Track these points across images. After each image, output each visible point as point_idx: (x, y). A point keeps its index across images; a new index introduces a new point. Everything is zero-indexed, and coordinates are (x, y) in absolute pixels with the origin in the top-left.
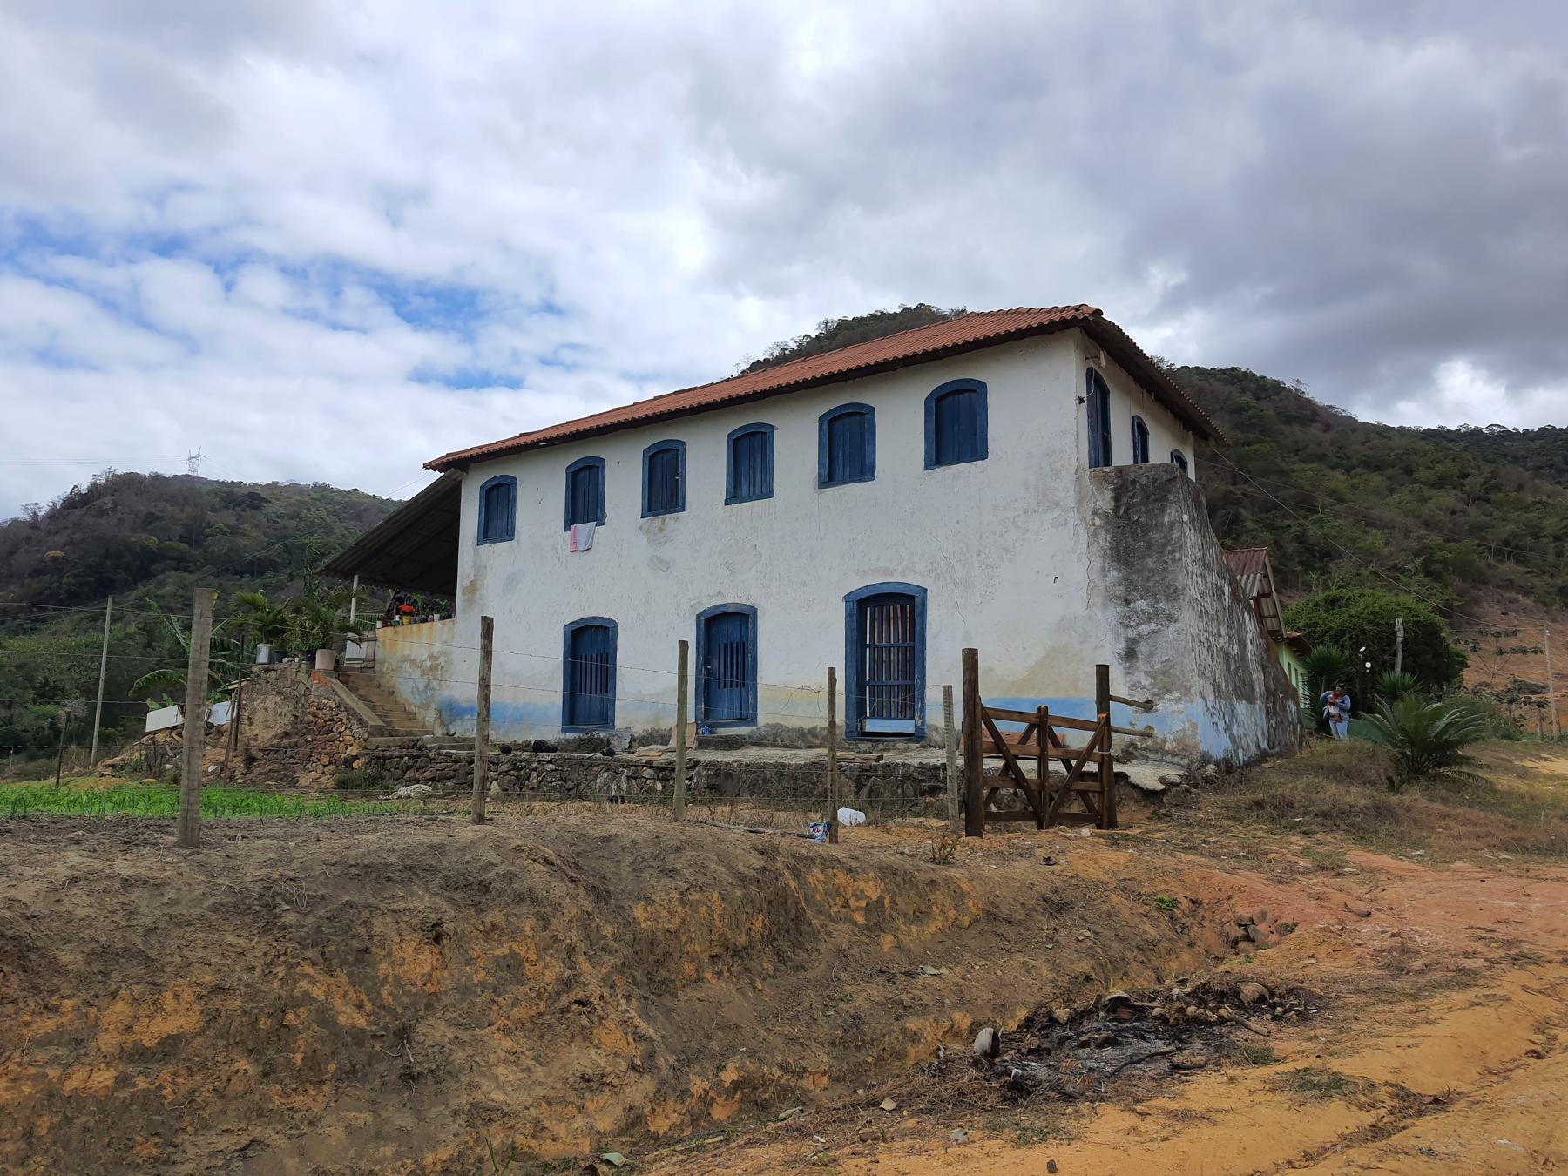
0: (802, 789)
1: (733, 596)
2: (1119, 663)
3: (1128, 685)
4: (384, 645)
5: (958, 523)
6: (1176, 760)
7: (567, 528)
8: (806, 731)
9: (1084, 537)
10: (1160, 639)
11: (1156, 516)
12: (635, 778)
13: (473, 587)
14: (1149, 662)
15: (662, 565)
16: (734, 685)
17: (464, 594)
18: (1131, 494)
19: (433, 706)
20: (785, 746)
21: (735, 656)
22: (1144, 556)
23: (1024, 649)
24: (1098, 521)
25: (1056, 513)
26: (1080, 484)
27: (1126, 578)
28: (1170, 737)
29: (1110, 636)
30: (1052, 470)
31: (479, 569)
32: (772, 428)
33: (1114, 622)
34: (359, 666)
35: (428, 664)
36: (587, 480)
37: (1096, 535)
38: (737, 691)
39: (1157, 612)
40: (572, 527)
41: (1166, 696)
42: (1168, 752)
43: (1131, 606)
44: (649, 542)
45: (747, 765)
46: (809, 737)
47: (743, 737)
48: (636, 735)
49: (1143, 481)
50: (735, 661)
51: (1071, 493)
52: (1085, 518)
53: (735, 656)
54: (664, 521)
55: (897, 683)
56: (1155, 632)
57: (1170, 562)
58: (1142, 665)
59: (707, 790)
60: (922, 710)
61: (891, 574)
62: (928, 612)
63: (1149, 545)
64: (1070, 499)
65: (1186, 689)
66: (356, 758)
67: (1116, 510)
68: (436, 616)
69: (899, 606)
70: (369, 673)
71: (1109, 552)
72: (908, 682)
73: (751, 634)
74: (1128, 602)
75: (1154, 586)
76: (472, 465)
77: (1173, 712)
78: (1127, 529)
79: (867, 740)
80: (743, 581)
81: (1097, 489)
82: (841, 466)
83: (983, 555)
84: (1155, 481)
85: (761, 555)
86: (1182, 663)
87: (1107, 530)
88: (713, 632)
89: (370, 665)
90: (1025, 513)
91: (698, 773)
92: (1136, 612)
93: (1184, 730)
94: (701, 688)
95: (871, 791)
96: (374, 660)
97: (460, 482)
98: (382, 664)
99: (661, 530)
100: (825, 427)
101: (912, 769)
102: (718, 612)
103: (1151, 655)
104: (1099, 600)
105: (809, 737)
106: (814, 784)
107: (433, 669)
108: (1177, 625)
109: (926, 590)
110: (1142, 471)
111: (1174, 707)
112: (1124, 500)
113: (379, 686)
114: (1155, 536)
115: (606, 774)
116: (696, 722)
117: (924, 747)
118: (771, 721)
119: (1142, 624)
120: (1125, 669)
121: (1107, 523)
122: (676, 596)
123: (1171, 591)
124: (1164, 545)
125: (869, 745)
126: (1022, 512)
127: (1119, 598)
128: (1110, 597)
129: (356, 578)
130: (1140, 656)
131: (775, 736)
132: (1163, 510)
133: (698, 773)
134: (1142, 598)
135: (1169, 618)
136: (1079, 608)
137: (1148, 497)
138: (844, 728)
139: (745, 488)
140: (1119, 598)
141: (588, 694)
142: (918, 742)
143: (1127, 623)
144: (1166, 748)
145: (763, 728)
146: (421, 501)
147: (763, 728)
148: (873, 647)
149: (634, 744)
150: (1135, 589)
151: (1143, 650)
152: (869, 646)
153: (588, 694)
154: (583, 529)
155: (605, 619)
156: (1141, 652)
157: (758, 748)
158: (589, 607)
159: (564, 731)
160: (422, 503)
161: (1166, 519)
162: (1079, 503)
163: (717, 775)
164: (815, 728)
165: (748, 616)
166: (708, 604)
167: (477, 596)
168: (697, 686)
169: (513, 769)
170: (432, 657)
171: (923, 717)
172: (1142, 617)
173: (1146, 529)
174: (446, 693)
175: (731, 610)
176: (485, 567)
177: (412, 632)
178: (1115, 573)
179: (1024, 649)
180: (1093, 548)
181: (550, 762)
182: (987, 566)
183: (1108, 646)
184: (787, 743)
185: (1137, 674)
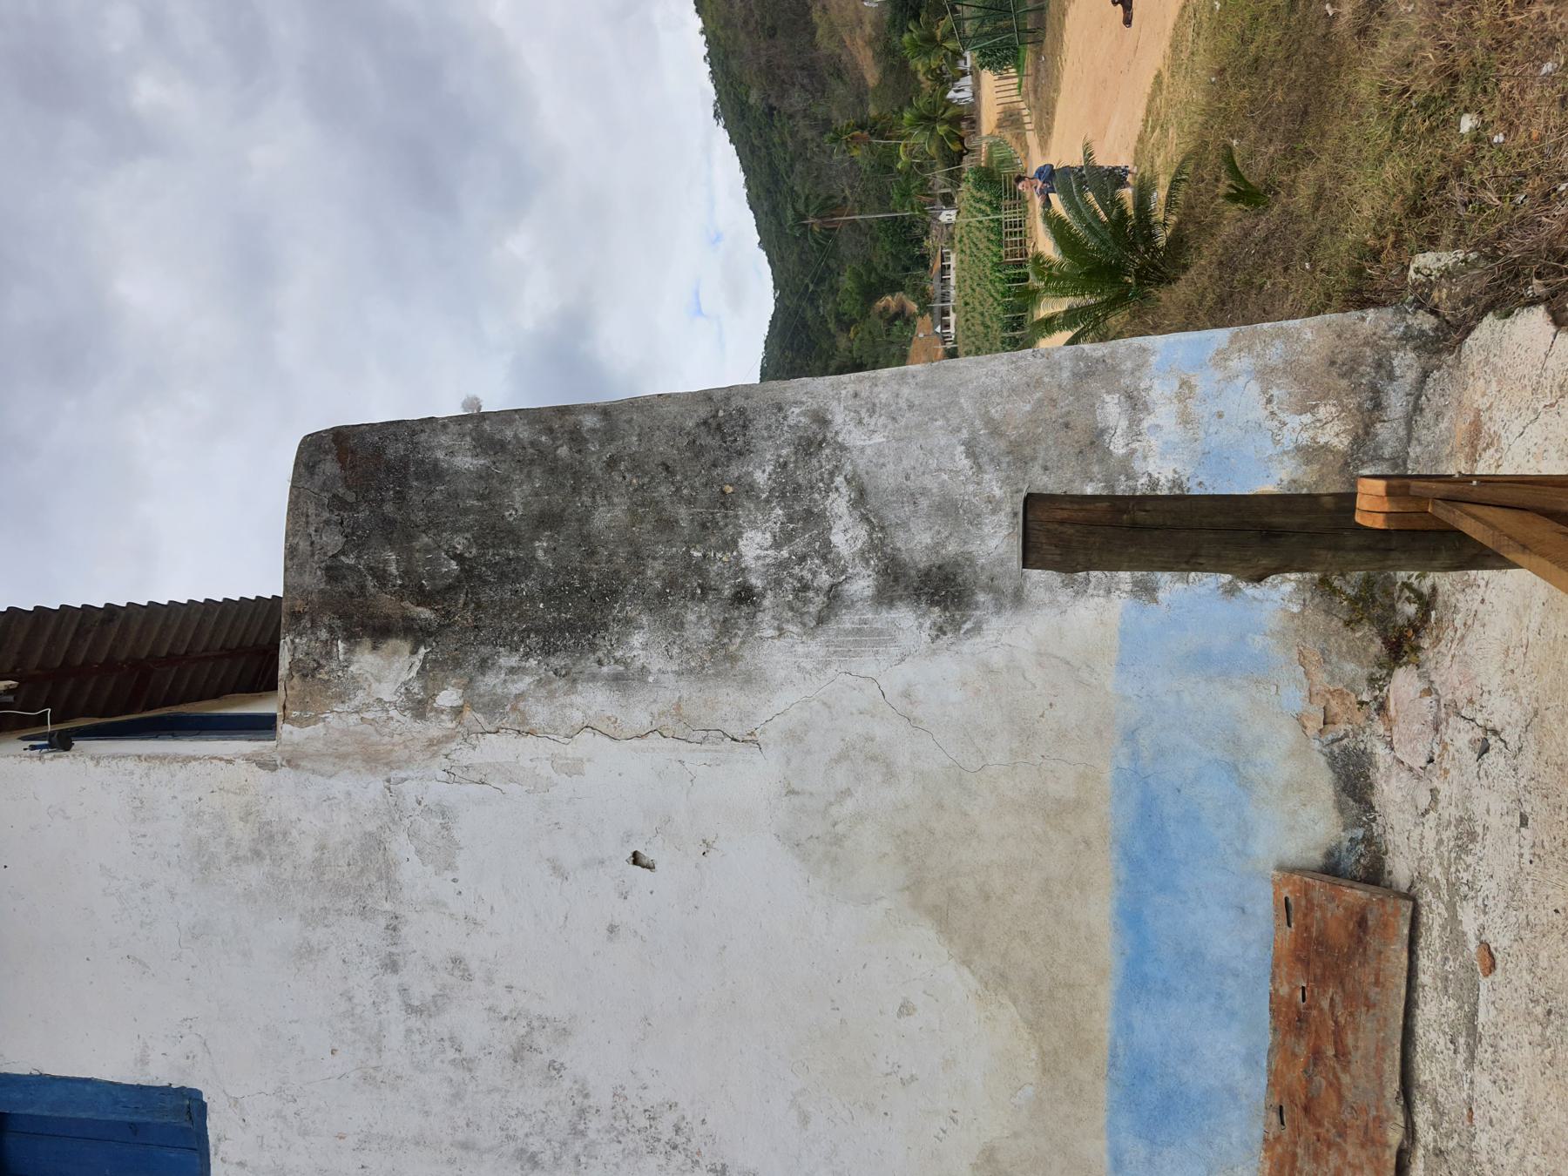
2: (977, 629)
6: (1396, 402)
9: (497, 748)
10: (888, 478)
11: (453, 496)
14: (976, 519)
18: (370, 583)
22: (586, 538)
23: (905, 1009)
24: (448, 697)
25: (400, 846)
26: (320, 756)
28: (1297, 428)
29: (868, 664)
30: (257, 854)
33: (816, 647)
37: (493, 706)
39: (787, 490)
41: (1118, 447)
42: (1363, 437)
43: (756, 582)
49: (332, 541)
51: (339, 785)
52: (431, 743)
56: (861, 497)
57: (611, 449)
63: (548, 520)
65: (1089, 374)
67: (417, 634)
71: (556, 661)
74: (745, 596)
75: (690, 502)
77: (1185, 420)
78: (486, 595)
81: (341, 697)
83: (535, 1144)
84: (338, 503)
86: (985, 394)
87: (484, 665)
90: (392, 965)
92: (782, 565)
93: (1265, 375)
103: (949, 510)
104: (727, 702)
108: (839, 417)
111: (1163, 415)
112: (387, 603)
119: (827, 544)
120: (999, 608)
121: (457, 664)
124: (554, 469)
126: (392, 980)
127: (726, 627)
130: (952, 548)
132: (434, 473)
134: (731, 544)
135: (809, 446)
137: (388, 523)
140: (726, 627)
143: (820, 600)
144: (1342, 443)
150: (699, 569)
151: (926, 539)
156: (936, 547)
161: (466, 462)
162: (373, 759)
172: (799, 545)
173: (494, 532)
178: (637, 639)
179: (905, 1009)
180: (539, 713)
182: (578, 1133)
183: (907, 670)
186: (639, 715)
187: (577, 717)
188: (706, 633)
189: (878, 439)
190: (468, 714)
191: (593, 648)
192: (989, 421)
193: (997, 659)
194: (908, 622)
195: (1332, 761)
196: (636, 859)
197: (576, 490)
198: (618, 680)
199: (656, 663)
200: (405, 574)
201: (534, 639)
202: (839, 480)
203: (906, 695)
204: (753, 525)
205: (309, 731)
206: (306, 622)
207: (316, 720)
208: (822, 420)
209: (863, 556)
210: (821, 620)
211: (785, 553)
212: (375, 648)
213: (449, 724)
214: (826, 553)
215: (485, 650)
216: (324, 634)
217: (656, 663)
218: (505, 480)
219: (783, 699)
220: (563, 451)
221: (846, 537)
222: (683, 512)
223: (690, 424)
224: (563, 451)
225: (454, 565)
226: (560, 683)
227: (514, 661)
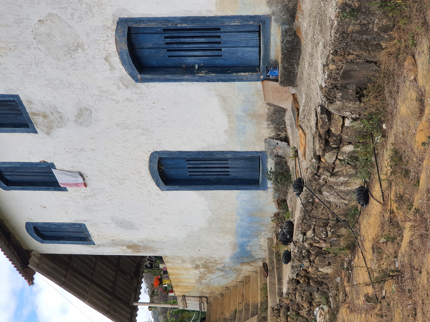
4: (188, 292)
12: (334, 168)
16: (218, 40)
17: (140, 252)
19: (238, 266)
21: (182, 40)
31: (115, 243)
34: (206, 305)
35: (202, 270)
36: (12, 174)
38: (224, 37)
40: (62, 186)
44: (61, 127)
45: (335, 53)
47: (285, 33)
48: (273, 134)
50: (188, 40)
53: (182, 40)
59: (364, 99)
68: (161, 266)
70: (211, 299)
73: (153, 25)
76: (24, 248)
80: (88, 35)
85: (50, 15)
88: (154, 63)
89: (204, 300)
91: (338, 110)
94: (221, 76)
96: (200, 297)
97: (41, 254)
99: (45, 116)
102: (129, 60)
107: (206, 266)
113: (222, 295)
115: (324, 193)
116: (263, 80)
122: (117, 102)
133: (338, 110)
141: (229, 162)
145: (274, 8)
146: (63, 279)
147: (274, 8)
149: (283, 135)
154: (61, 178)
155: (150, 161)
157: (299, 14)
158: (140, 173)
159: (265, 188)
160: (65, 277)
163: (344, 87)
165: (129, 28)
167: (140, 244)
168: (218, 81)
169: (309, 258)
170: (197, 267)
174: (227, 260)
175: (125, 47)
176: (113, 240)
177: (174, 274)
181: (304, 234)
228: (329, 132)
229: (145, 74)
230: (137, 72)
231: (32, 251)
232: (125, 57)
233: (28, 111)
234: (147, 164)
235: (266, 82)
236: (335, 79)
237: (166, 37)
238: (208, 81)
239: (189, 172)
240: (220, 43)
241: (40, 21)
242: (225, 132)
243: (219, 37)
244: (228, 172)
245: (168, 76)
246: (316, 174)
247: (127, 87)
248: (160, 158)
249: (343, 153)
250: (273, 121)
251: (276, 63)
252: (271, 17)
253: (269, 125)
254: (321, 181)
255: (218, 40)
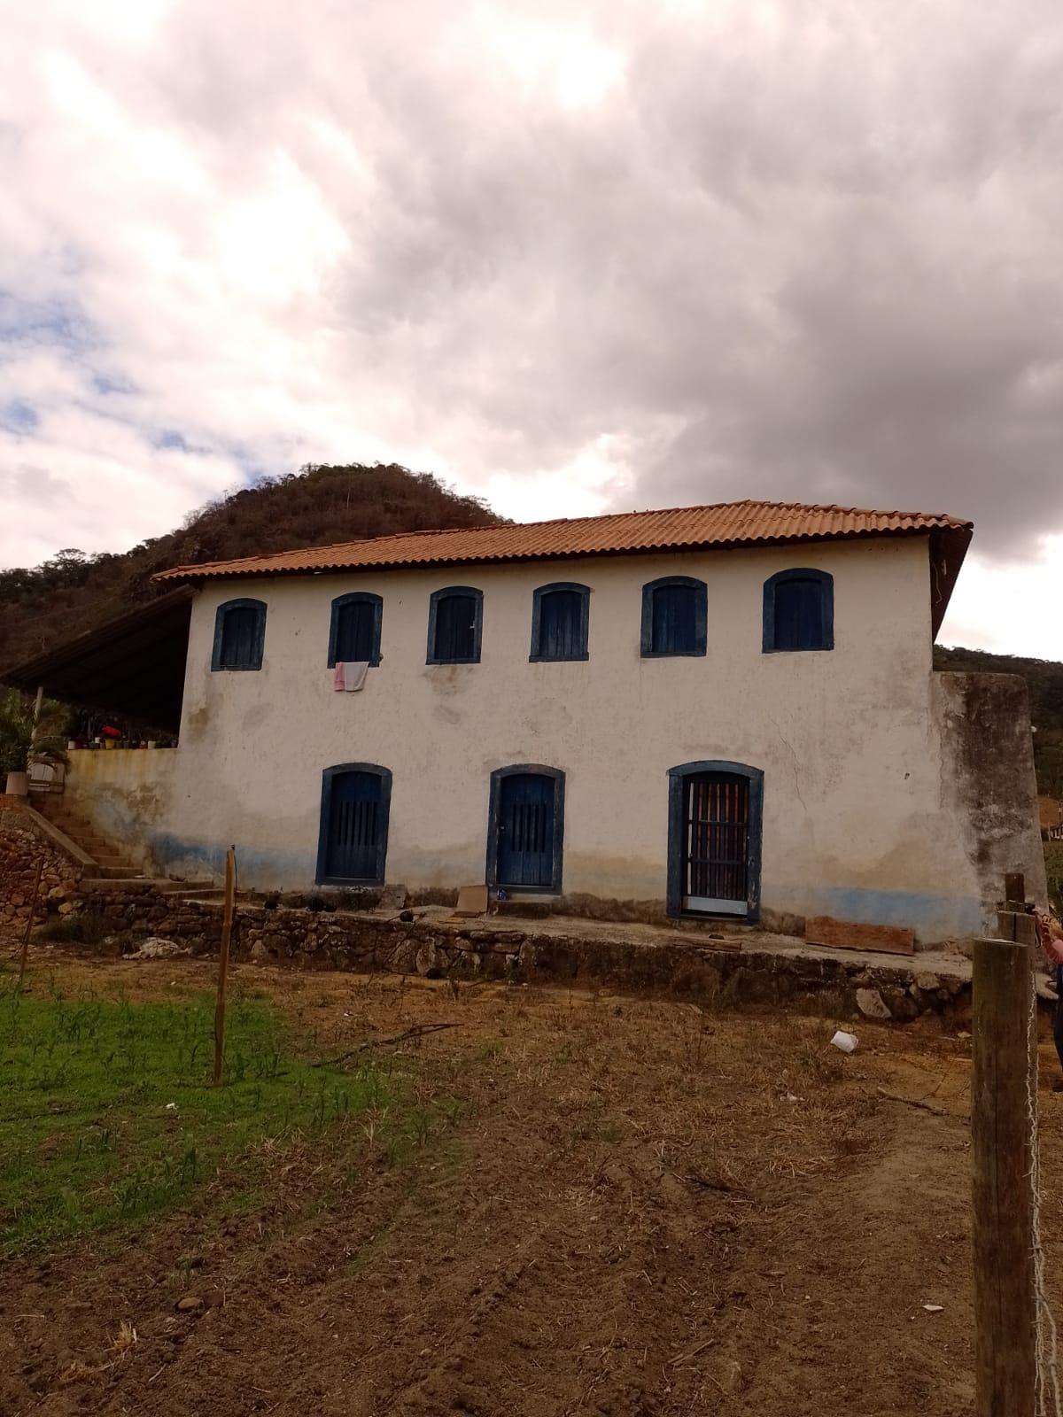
0: (658, 974)
1: (537, 755)
3: (981, 885)
5: (799, 709)
7: (331, 664)
8: (620, 905)
9: (937, 739)
13: (203, 716)
14: (1003, 865)
15: (454, 717)
16: (532, 848)
17: (191, 721)
20: (595, 918)
23: (872, 841)
24: (950, 724)
27: (978, 782)
29: (962, 836)
30: (904, 669)
31: (213, 697)
32: (588, 590)
33: (967, 824)
34: (42, 790)
35: (139, 795)
37: (948, 736)
39: (1009, 818)
40: (339, 665)
43: (984, 809)
46: (624, 910)
48: (411, 893)
49: (995, 690)
54: (454, 670)
55: (721, 862)
56: (1008, 837)
57: (1021, 770)
58: (996, 868)
60: (757, 893)
61: (723, 752)
62: (766, 795)
63: (1001, 752)
64: (925, 700)
65: (1039, 893)
66: (63, 900)
67: (968, 714)
68: (151, 743)
69: (727, 786)
71: (961, 754)
72: (736, 863)
74: (980, 805)
75: (1006, 792)
79: (692, 919)
81: (949, 692)
82: (665, 637)
87: (959, 733)
89: (57, 789)
90: (874, 707)
91: (526, 949)
92: (989, 815)
95: (740, 981)
97: (191, 599)
98: (75, 789)
100: (650, 596)
101: (788, 962)
102: (518, 772)
103: (1004, 859)
105: (624, 910)
106: (671, 969)
107: (145, 801)
108: (1029, 832)
109: (763, 772)
110: (993, 680)
112: (976, 706)
113: (69, 814)
114: (1007, 744)
115: (409, 942)
117: (758, 930)
118: (579, 891)
119: (994, 827)
120: (978, 870)
121: (960, 726)
123: (1023, 798)
125: (694, 923)
126: (870, 707)
127: (971, 800)
128: (962, 799)
129: (40, 691)
130: (994, 859)
131: (583, 907)
132: (1014, 720)
135: (1022, 824)
136: (931, 806)
138: (665, 905)
139: (552, 647)
140: (971, 800)
142: (751, 925)
145: (569, 898)
147: (569, 898)
148: (695, 822)
152: (690, 822)
153: (349, 844)
154: (352, 669)
159: (319, 881)
161: (1017, 729)
162: (933, 703)
163: (549, 951)
164: (631, 901)
165: (554, 779)
166: (506, 763)
169: (284, 929)
171: (757, 900)
172: (994, 820)
174: (161, 829)
175: (533, 772)
176: (221, 695)
178: (967, 776)
179: (872, 841)
180: (947, 749)
181: (334, 923)
184: (597, 914)
185: (989, 875)
186: (946, 777)
187: (946, 760)
188: (970, 795)
189: (1023, 842)
190: (946, 730)
191: (965, 764)
192: (1028, 869)
193: (965, 868)
194: (974, 847)
195: (941, 943)
196: (908, 775)
197: (1009, 760)
198: (956, 771)
199: (961, 781)
200: (985, 711)
201: (967, 747)
202: (1012, 831)
203: (955, 846)
204: (1000, 808)
205: (939, 682)
206: (970, 681)
207: (942, 685)
208: (1029, 827)
209: (991, 836)
210: (974, 825)
211: (992, 816)
212: (963, 702)
213: (942, 724)
214: (992, 827)
215: (964, 734)
216: (967, 687)
217: (961, 781)
218: (1013, 740)
219: (953, 816)
220: (1020, 757)
221: (996, 832)
222: (1004, 789)
223: (1028, 792)
224: (1020, 757)
225: (987, 725)
226: (954, 755)
227: (961, 742)
228: (497, 941)
229: (501, 782)
230: (504, 776)
231: (201, 590)
232: (522, 769)
233: (458, 665)
234: (372, 762)
235: (486, 889)
236: (559, 945)
237: (537, 806)
238: (489, 837)
239: (348, 804)
240: (528, 849)
241: (565, 708)
242: (417, 847)
243: (535, 850)
244: (345, 843)
245: (497, 802)
246: (437, 933)
247: (485, 763)
248: (381, 777)
249: (471, 956)
250: (429, 893)
251: (508, 898)
252: (558, 894)
253: (425, 889)
254: (428, 938)
255: (532, 848)
